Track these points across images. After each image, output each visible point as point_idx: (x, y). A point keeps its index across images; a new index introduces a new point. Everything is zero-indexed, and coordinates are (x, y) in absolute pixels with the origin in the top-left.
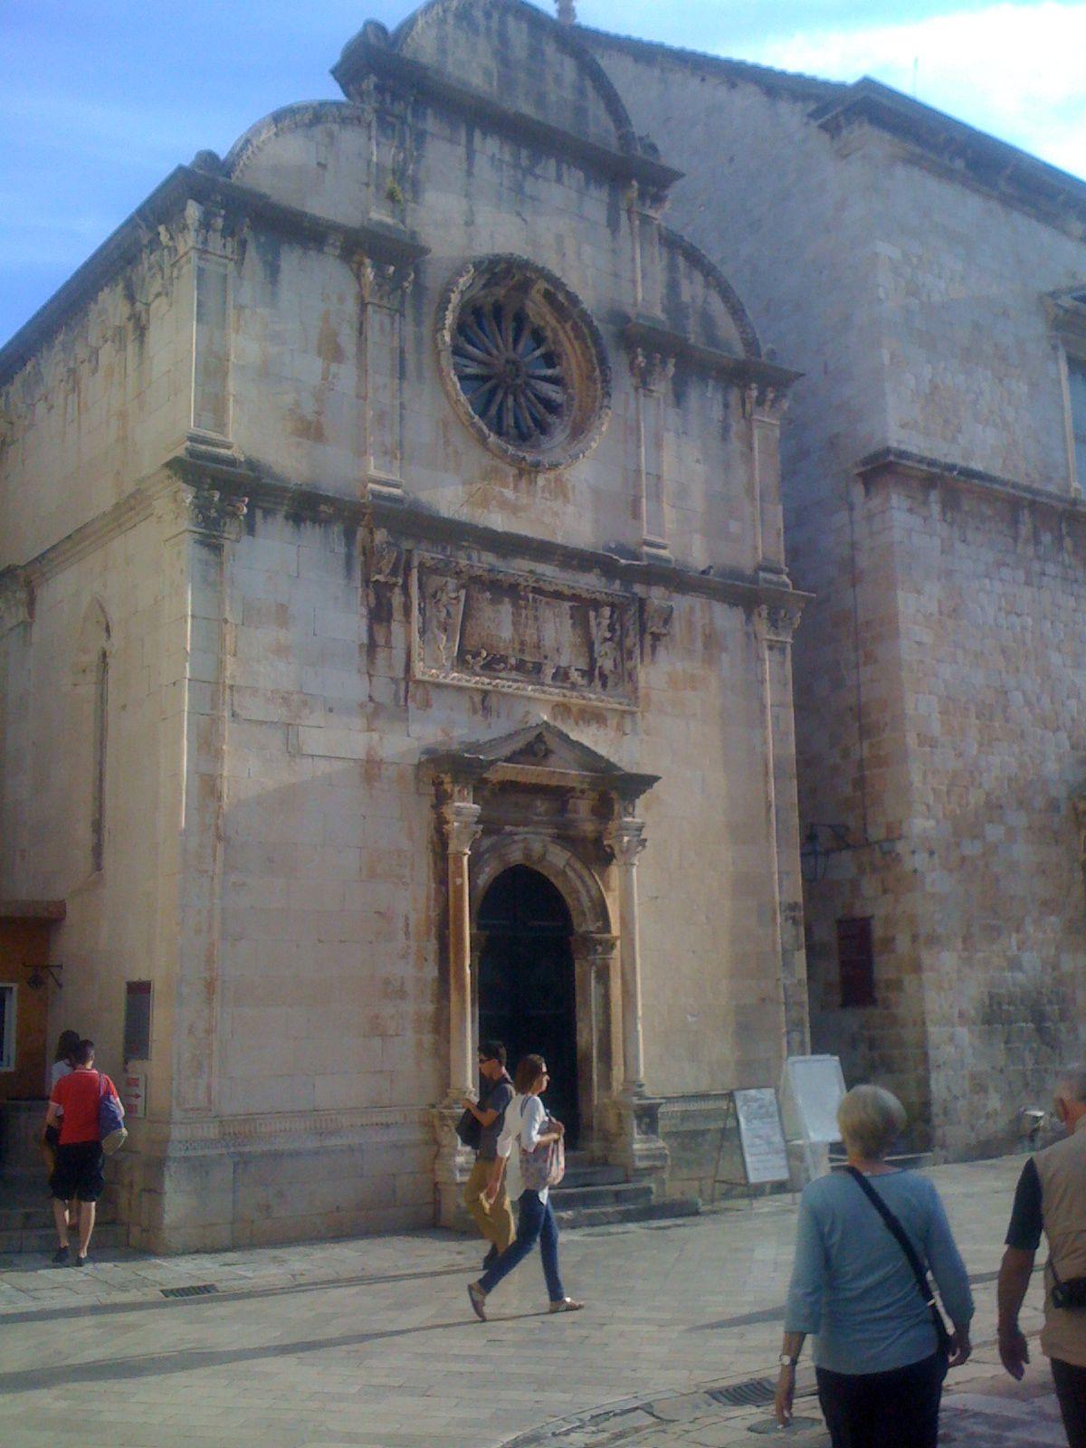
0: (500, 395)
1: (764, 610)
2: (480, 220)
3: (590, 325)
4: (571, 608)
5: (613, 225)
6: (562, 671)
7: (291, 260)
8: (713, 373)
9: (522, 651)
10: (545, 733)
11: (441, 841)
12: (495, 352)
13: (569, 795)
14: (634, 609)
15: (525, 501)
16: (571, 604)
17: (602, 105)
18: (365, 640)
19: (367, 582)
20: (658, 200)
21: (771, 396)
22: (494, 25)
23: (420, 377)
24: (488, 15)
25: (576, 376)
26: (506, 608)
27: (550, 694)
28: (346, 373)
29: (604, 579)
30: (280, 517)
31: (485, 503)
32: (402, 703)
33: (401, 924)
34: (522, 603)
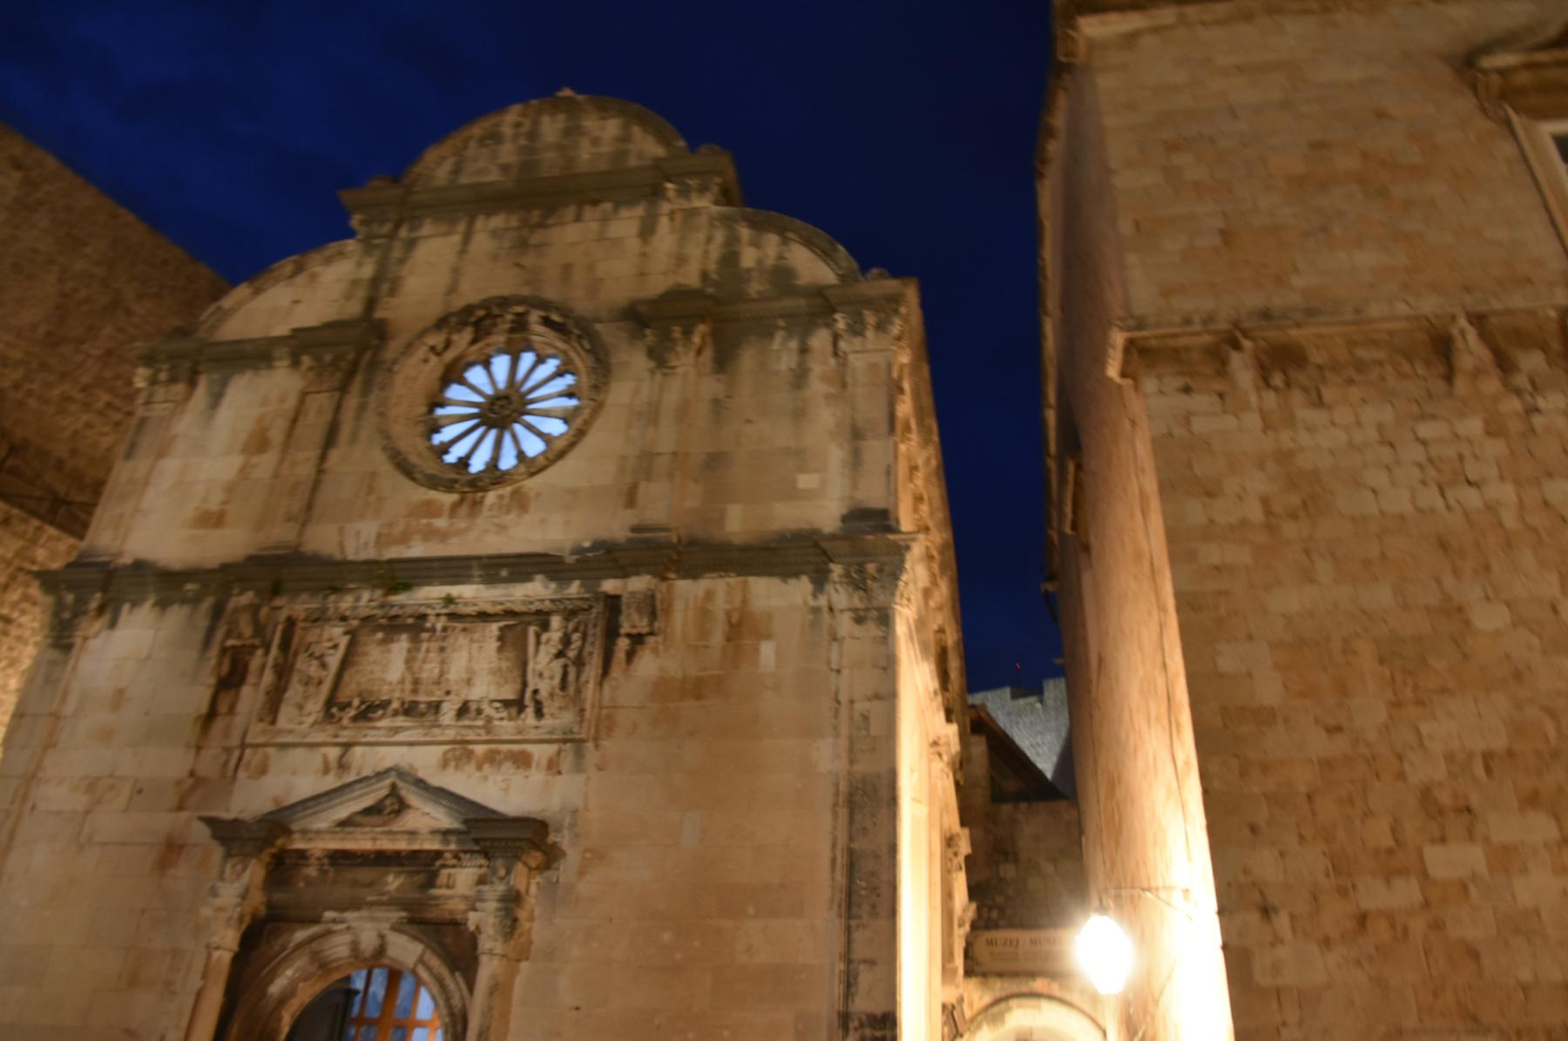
4: (501, 629)
8: (781, 323)
9: (415, 691)
10: (400, 784)
13: (438, 863)
14: (598, 609)
16: (502, 624)
18: (204, 709)
19: (224, 650)
21: (870, 318)
29: (553, 585)
31: (404, 539)
32: (230, 773)
34: (425, 635)
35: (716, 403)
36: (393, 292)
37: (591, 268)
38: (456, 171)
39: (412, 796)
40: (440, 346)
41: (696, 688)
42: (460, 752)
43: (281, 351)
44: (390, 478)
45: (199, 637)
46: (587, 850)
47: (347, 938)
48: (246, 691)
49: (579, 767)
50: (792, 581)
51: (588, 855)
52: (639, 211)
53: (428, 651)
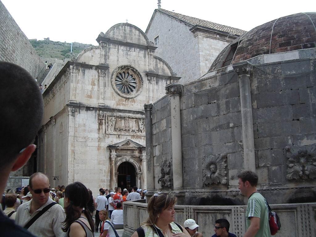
0: (124, 86)
2: (120, 60)
3: (139, 74)
5: (145, 57)
7: (87, 71)
11: (110, 158)
12: (123, 80)
18: (98, 128)
19: (99, 119)
20: (153, 52)
22: (123, 28)
23: (108, 86)
24: (122, 27)
26: (123, 121)
28: (96, 88)
30: (84, 110)
33: (104, 171)
34: (126, 120)
35: (157, 90)
36: (108, 58)
37: (138, 62)
38: (114, 34)
43: (94, 68)
44: (115, 94)
45: (94, 117)
47: (125, 159)
48: (103, 126)
52: (143, 52)
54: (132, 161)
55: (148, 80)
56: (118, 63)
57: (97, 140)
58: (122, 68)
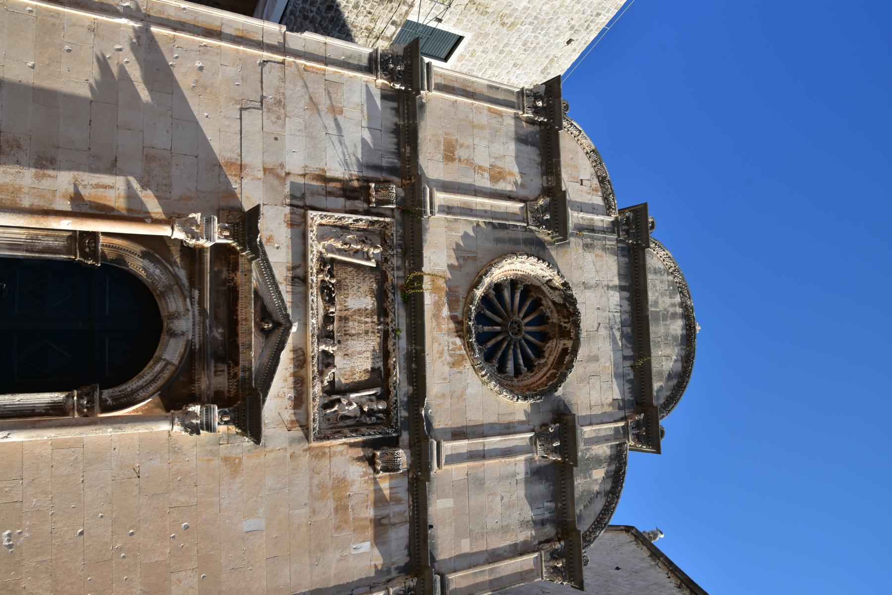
1: (412, 583)
2: (588, 293)
4: (379, 368)
6: (330, 360)
8: (559, 505)
15: (443, 327)
16: (382, 369)
17: (668, 393)
18: (328, 174)
19: (368, 180)
25: (525, 383)
27: (312, 343)
29: (406, 399)
31: (435, 289)
34: (375, 318)
36: (587, 246)
38: (656, 272)
39: (275, 338)
40: (550, 284)
41: (341, 508)
42: (300, 360)
45: (376, 161)
46: (240, 459)
49: (292, 441)
50: (406, 552)
51: (237, 461)
53: (366, 323)
54: (172, 352)
55: (545, 425)
56: (577, 285)
57: (271, 162)
58: (568, 307)
